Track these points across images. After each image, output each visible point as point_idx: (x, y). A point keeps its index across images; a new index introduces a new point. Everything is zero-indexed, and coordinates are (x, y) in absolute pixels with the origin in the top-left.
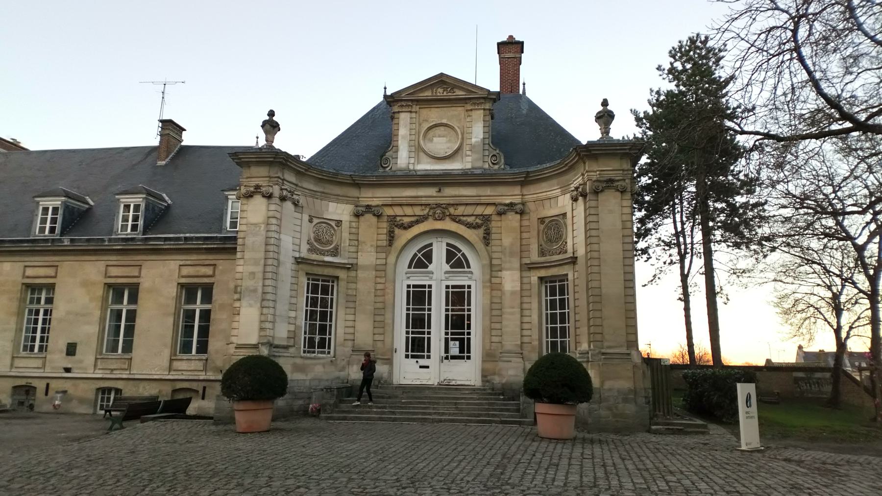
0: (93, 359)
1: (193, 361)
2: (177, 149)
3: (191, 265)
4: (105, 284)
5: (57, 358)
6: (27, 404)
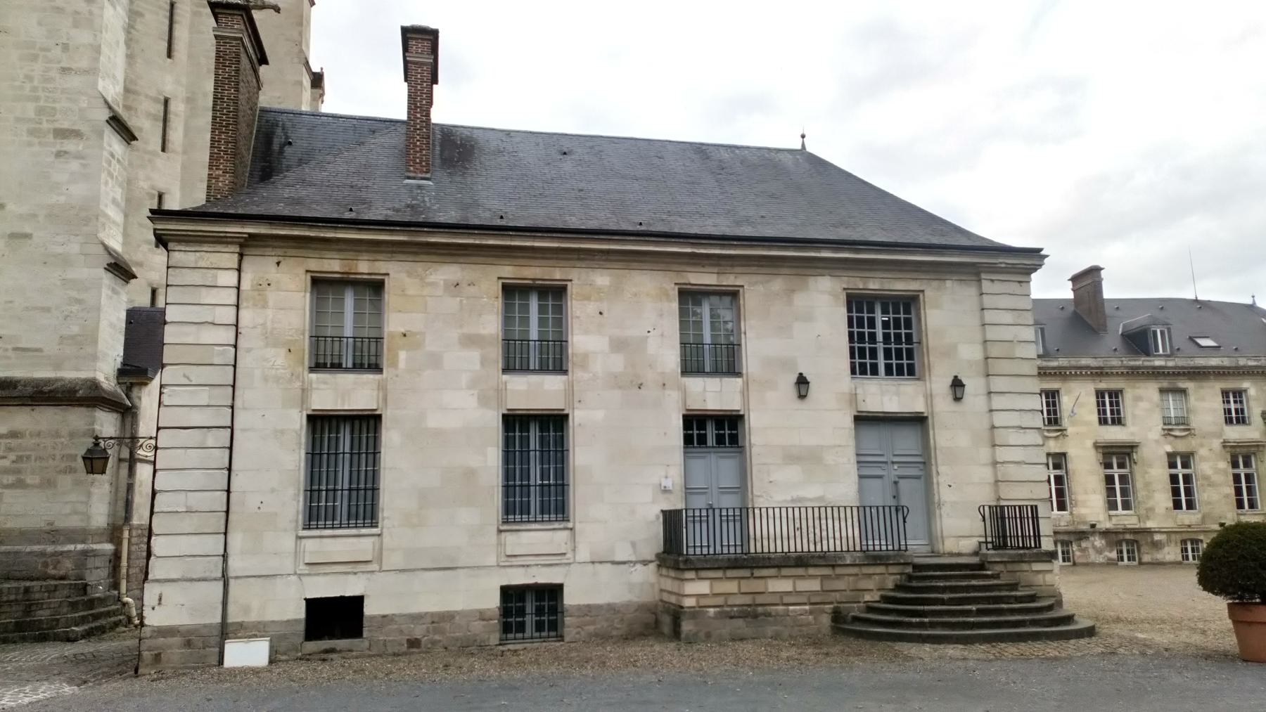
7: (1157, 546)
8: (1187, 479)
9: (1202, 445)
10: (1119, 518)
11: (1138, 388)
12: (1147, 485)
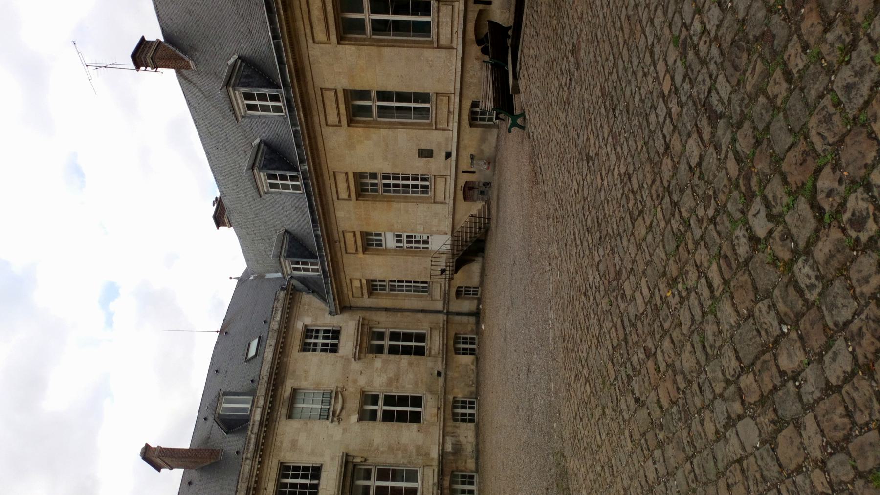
0: (436, 133)
1: (440, 19)
2: (170, 47)
3: (312, 28)
4: (348, 126)
5: (435, 165)
6: (483, 189)
7: (458, 449)
8: (390, 400)
9: (355, 381)
10: (425, 490)
11: (281, 443)
12: (391, 449)
